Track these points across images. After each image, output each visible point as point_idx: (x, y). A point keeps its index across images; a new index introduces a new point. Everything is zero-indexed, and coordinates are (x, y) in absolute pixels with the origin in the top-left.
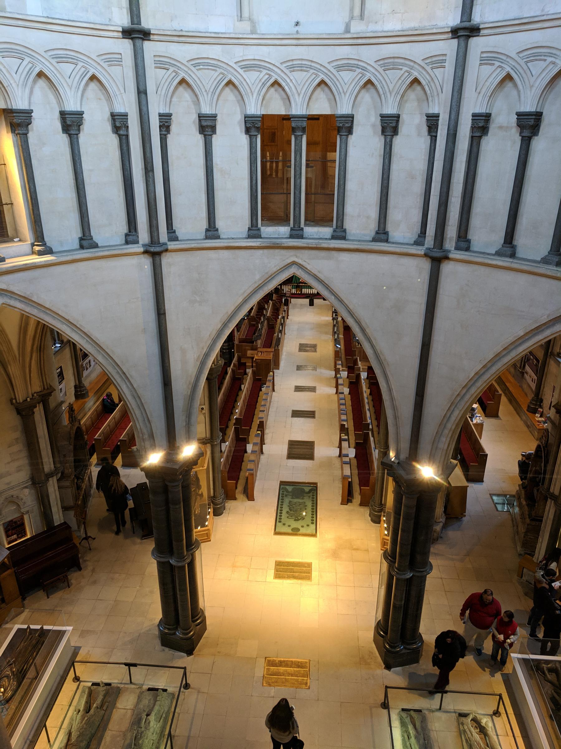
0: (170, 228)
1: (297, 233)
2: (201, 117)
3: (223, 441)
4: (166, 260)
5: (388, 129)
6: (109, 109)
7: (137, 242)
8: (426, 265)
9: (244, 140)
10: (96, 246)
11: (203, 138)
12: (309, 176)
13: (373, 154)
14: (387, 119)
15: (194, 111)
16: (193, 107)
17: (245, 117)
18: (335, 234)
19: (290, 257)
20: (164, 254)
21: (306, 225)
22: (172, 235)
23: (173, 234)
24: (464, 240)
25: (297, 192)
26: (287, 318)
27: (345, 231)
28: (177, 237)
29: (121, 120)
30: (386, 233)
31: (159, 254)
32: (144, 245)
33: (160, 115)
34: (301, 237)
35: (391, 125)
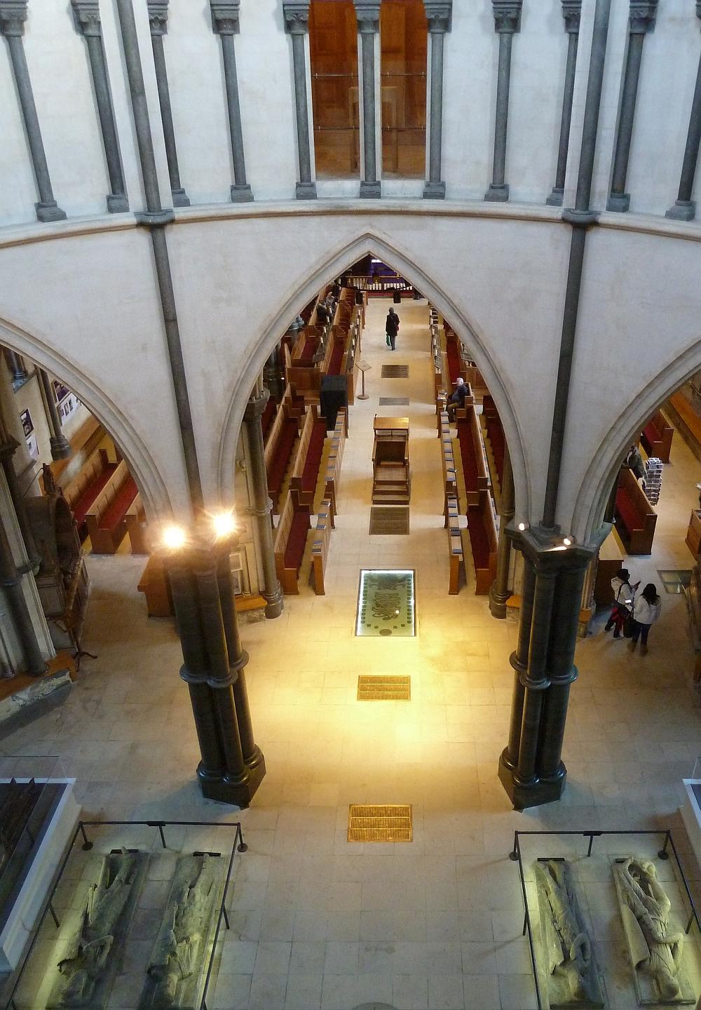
0: (176, 186)
1: (371, 190)
4: (173, 236)
7: (126, 209)
8: (565, 236)
9: (283, 42)
10: (62, 216)
11: (220, 40)
12: (386, 100)
17: (284, 5)
18: (428, 190)
19: (360, 226)
20: (168, 227)
21: (383, 177)
24: (620, 195)
25: (369, 126)
27: (443, 185)
29: (88, 12)
30: (505, 187)
31: (161, 226)
32: (136, 214)
34: (377, 195)
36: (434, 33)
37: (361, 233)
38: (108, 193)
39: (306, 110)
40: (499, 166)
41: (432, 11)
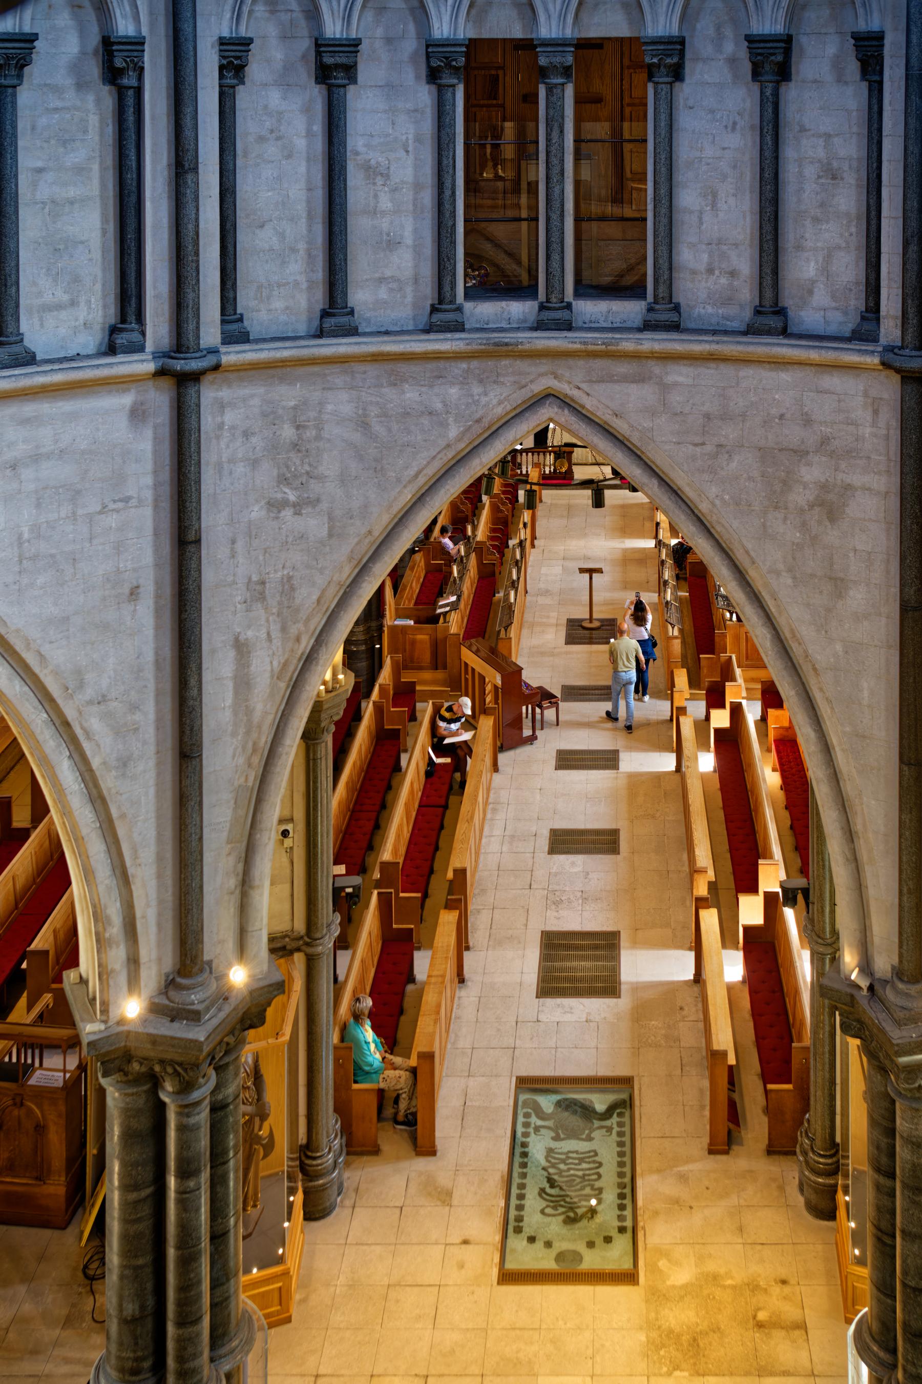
0: (230, 310)
2: (320, 45)
3: (344, 943)
4: (210, 394)
5: (767, 67)
6: (101, 29)
7: (141, 349)
9: (425, 96)
10: (30, 359)
11: (325, 93)
12: (586, 174)
13: (735, 123)
14: (762, 45)
15: (305, 33)
16: (303, 23)
17: (428, 46)
18: (653, 316)
20: (210, 377)
21: (578, 294)
22: (235, 331)
23: (234, 326)
25: (555, 216)
26: (533, 546)
27: (677, 308)
28: (247, 334)
29: (126, 54)
30: (781, 312)
31: (195, 377)
33: (222, 42)
35: (773, 58)
36: (657, 83)
37: (538, 387)
38: (113, 321)
39: (454, 193)
40: (768, 280)
41: (654, 53)
